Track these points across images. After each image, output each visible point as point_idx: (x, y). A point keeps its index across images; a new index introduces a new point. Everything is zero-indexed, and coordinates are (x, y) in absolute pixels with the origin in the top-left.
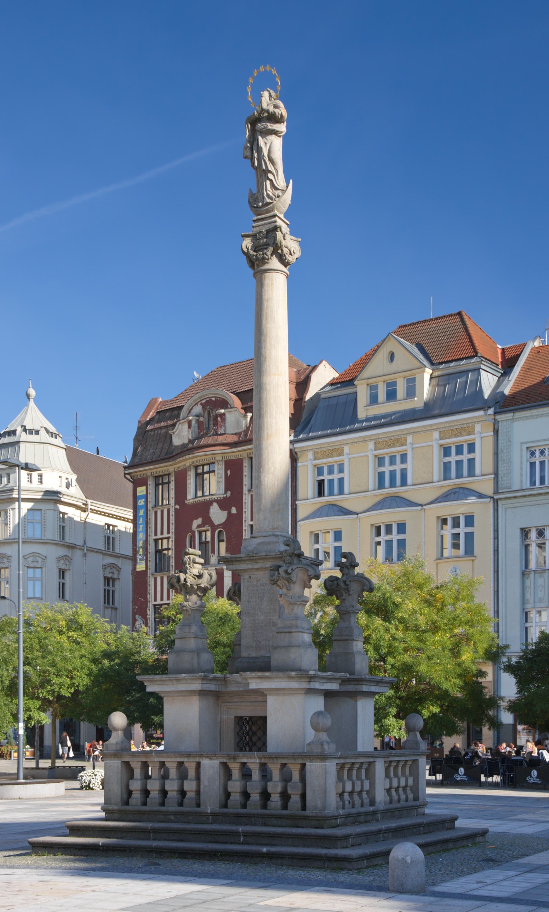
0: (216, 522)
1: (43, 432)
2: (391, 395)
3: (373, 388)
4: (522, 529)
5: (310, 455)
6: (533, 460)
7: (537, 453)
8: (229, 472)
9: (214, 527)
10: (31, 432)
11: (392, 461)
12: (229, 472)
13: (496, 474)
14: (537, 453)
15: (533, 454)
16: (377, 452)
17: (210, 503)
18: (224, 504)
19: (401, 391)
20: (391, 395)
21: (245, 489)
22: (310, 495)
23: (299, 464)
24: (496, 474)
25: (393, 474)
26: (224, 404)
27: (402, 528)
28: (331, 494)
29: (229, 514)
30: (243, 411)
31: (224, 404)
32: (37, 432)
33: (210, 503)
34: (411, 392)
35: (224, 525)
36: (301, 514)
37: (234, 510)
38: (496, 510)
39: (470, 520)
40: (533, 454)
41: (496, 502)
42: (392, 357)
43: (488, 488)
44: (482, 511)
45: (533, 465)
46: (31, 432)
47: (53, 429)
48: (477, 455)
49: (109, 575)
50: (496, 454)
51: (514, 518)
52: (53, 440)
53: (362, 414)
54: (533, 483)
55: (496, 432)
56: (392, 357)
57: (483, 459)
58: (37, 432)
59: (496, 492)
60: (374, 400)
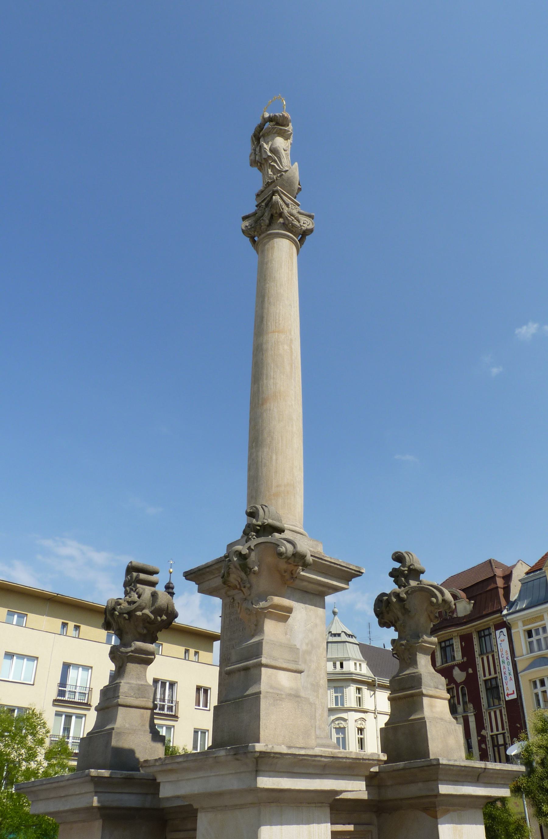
0: (459, 681)
1: (343, 635)
5: (520, 624)
8: (463, 644)
9: (457, 685)
10: (335, 635)
12: (463, 644)
17: (452, 667)
18: (462, 667)
21: (477, 654)
22: (525, 652)
23: (513, 631)
28: (540, 649)
29: (467, 673)
30: (468, 600)
32: (339, 635)
33: (452, 667)
35: (464, 682)
37: (470, 671)
46: (335, 635)
47: (349, 632)
52: (350, 640)
58: (339, 635)
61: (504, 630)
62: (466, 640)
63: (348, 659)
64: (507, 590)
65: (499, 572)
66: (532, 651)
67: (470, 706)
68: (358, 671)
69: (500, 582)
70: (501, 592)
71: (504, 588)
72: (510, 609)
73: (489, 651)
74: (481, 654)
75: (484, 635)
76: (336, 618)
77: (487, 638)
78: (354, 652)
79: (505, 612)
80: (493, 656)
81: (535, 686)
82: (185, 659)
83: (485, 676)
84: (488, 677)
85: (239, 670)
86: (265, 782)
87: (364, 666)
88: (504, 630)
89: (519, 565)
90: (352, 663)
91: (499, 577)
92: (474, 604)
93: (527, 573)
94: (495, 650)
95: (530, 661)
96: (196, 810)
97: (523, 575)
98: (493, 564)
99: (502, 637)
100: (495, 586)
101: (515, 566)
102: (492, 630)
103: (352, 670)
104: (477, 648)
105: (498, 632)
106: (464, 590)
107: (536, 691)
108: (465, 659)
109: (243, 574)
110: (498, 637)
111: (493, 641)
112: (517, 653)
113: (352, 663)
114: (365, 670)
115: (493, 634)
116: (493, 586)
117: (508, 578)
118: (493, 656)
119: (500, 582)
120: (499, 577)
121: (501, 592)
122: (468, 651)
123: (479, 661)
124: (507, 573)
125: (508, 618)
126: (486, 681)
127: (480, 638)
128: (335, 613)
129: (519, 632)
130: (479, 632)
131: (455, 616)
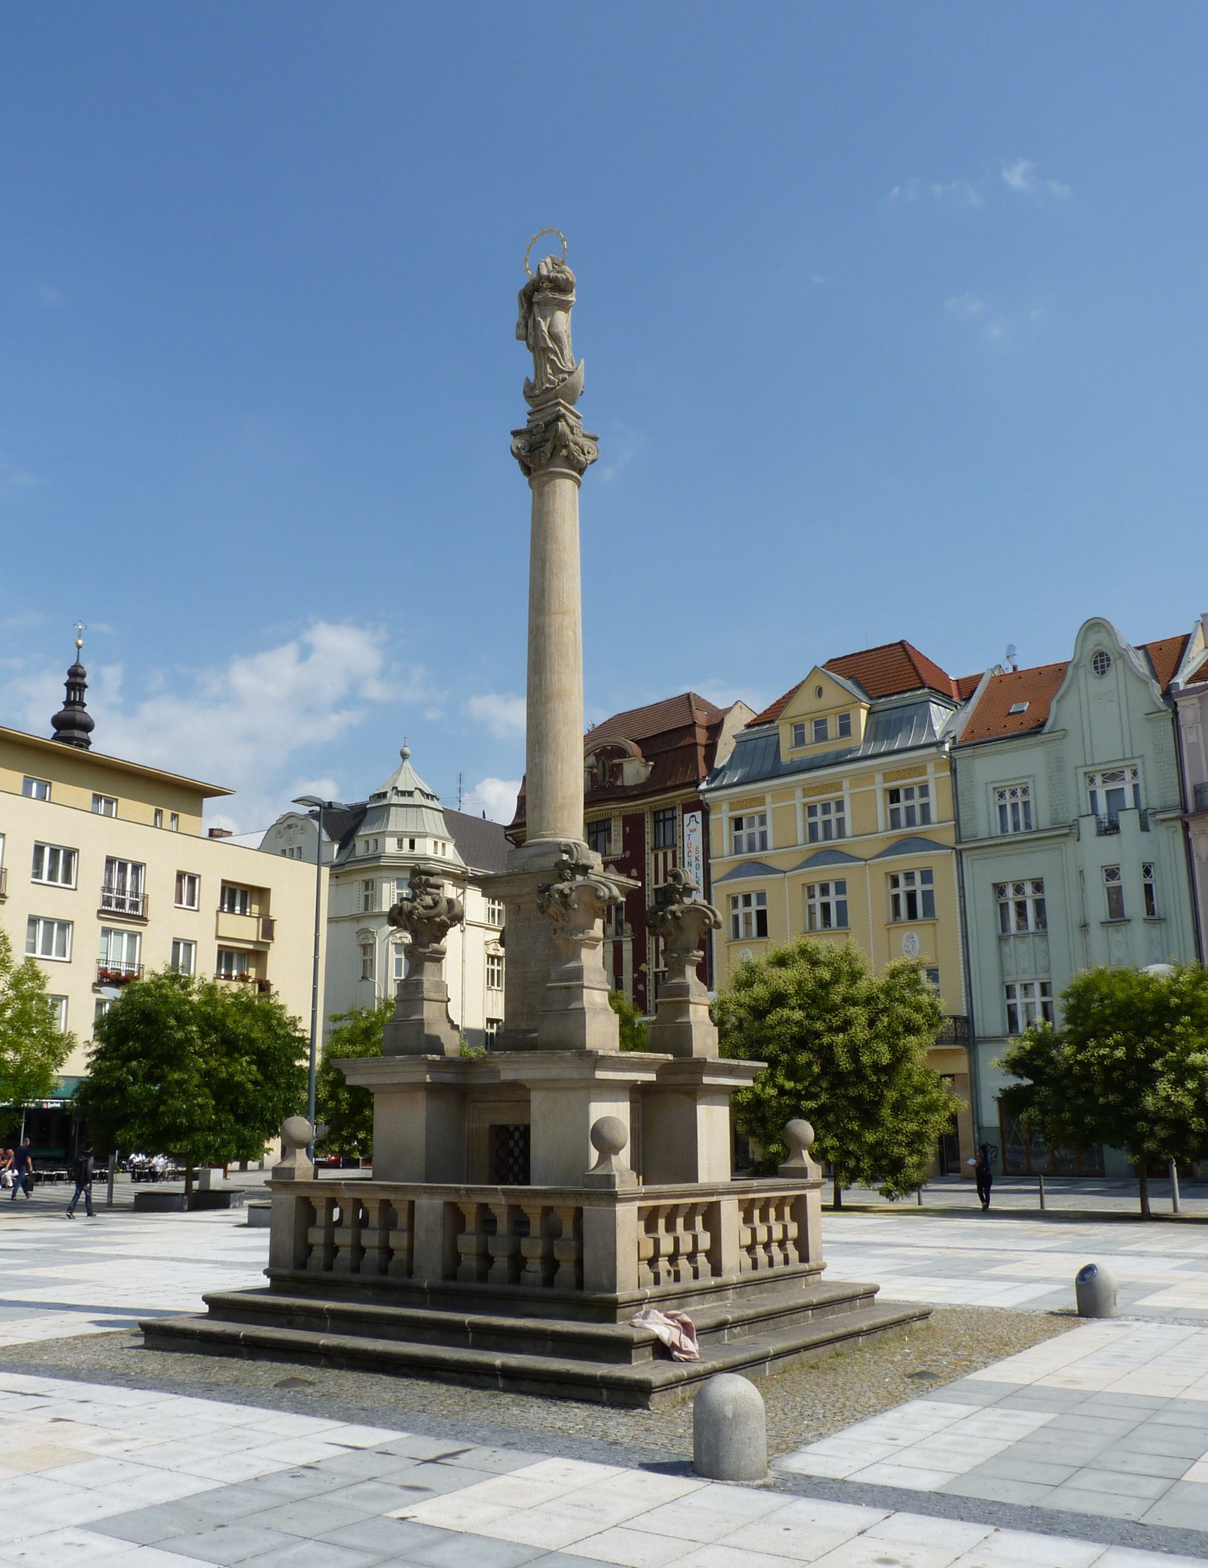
1: (417, 793)
2: (821, 735)
3: (799, 728)
4: (995, 885)
5: (725, 807)
6: (1002, 802)
7: (1008, 795)
10: (403, 793)
11: (826, 809)
13: (957, 820)
14: (1008, 795)
15: (1002, 795)
16: (807, 800)
19: (833, 727)
20: (821, 735)
21: (648, 848)
22: (726, 851)
23: (712, 817)
24: (957, 820)
25: (827, 824)
26: (622, 753)
27: (841, 887)
30: (643, 760)
31: (622, 753)
32: (410, 794)
34: (845, 730)
36: (714, 875)
38: (960, 863)
39: (927, 876)
40: (1002, 795)
41: (959, 853)
43: (949, 838)
44: (943, 865)
45: (1002, 808)
46: (403, 793)
47: (428, 791)
48: (932, 799)
49: (493, 953)
50: (955, 797)
51: (983, 874)
52: (429, 803)
53: (786, 757)
55: (954, 771)
57: (940, 804)
58: (410, 794)
59: (959, 841)
60: (800, 740)
61: (698, 814)
62: (634, 824)
63: (424, 835)
64: (711, 749)
65: (701, 718)
66: (738, 851)
67: (628, 927)
68: (439, 855)
69: (701, 736)
70: (701, 751)
71: (706, 746)
72: (712, 782)
73: (669, 844)
74: (656, 848)
75: (665, 819)
76: (407, 763)
77: (668, 824)
78: (435, 823)
79: (703, 786)
80: (674, 853)
81: (735, 906)
82: (155, 826)
83: (657, 882)
84: (661, 884)
85: (561, 988)
86: (600, 1075)
87: (450, 847)
88: (698, 814)
89: (737, 708)
90: (430, 842)
91: (701, 726)
92: (653, 767)
93: (748, 726)
94: (679, 844)
95: (733, 866)
96: (529, 1090)
97: (740, 729)
98: (693, 703)
99: (693, 825)
100: (691, 741)
101: (730, 709)
102: (679, 812)
103: (430, 852)
104: (649, 839)
105: (687, 816)
106: (637, 742)
107: (735, 912)
108: (628, 854)
109: (562, 909)
110: (686, 823)
111: (679, 829)
112: (713, 853)
113: (430, 842)
114: (451, 854)
115: (679, 819)
116: (688, 741)
117: (715, 729)
118: (674, 853)
119: (701, 736)
120: (701, 726)
121: (701, 751)
122: (633, 842)
123: (650, 858)
124: (715, 721)
125: (708, 796)
126: (657, 891)
127: (656, 822)
128: (404, 756)
129: (721, 819)
130: (656, 814)
131: (619, 783)
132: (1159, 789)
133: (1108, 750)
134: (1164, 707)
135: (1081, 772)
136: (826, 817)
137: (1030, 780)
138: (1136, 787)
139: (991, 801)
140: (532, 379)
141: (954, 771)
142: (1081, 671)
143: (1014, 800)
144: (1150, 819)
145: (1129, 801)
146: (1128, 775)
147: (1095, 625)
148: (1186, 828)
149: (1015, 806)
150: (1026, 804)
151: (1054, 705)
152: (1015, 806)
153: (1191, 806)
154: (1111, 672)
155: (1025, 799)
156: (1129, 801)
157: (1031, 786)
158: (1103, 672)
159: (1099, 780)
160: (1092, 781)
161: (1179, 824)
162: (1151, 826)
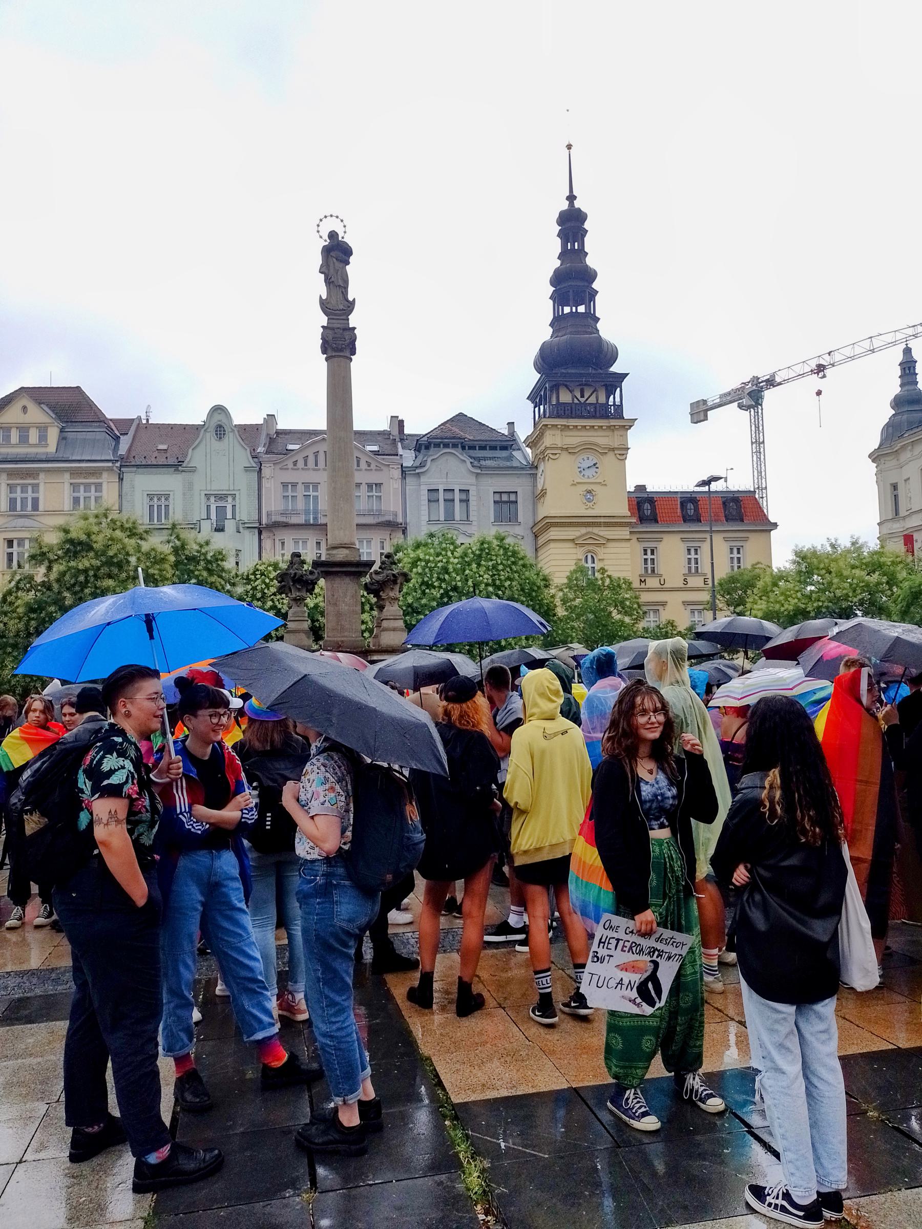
2: (24, 439)
6: (151, 503)
20: (24, 439)
42: (25, 409)
54: (151, 519)
55: (121, 479)
56: (25, 409)
132: (246, 511)
133: (220, 486)
134: (254, 465)
135: (203, 493)
136: (24, 495)
137: (171, 493)
138: (234, 506)
139: (145, 503)
140: (324, 297)
141: (121, 479)
142: (208, 435)
143: (159, 503)
144: (241, 526)
145: (229, 516)
146: (230, 499)
147: (219, 410)
148: (260, 533)
149: (159, 507)
150: (167, 506)
151: (190, 450)
152: (159, 507)
153: (264, 521)
154: (226, 440)
155: (167, 503)
156: (229, 516)
157: (171, 496)
158: (220, 438)
159: (212, 499)
160: (208, 499)
161: (256, 531)
162: (241, 530)
